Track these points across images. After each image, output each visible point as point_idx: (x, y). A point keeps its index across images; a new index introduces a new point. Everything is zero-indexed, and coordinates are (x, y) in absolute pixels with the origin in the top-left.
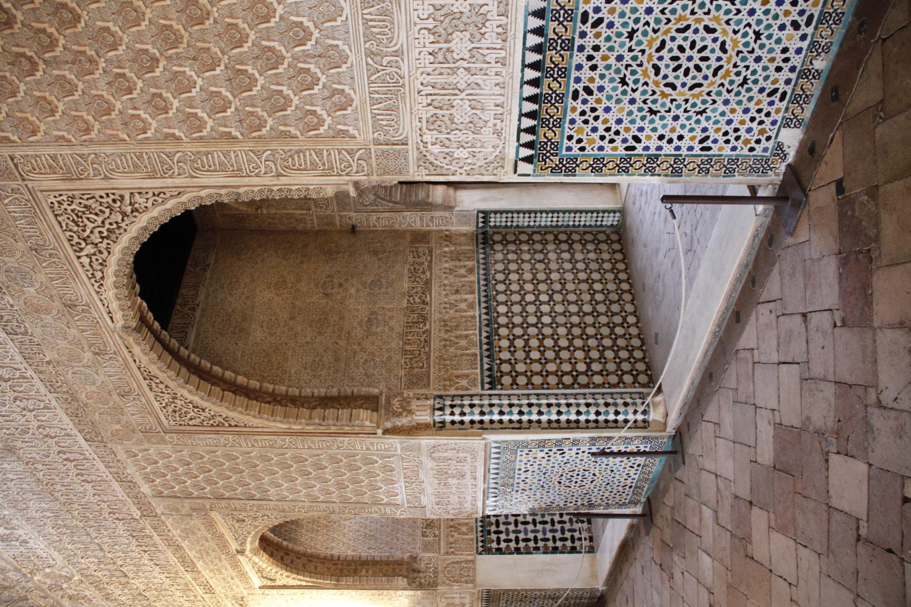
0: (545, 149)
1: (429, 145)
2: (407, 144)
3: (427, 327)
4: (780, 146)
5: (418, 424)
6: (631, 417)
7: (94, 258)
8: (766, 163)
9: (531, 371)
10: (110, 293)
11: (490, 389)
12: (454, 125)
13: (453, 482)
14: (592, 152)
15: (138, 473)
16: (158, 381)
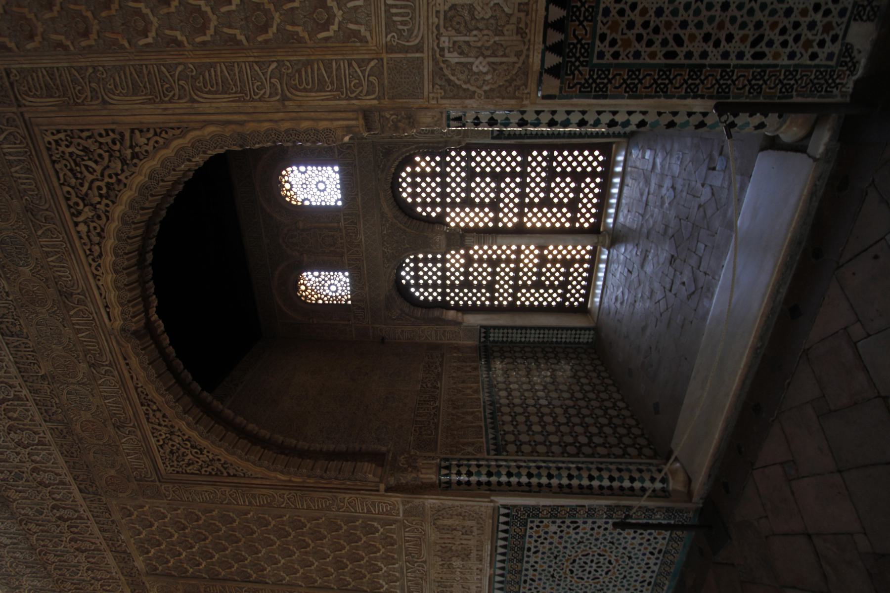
0: (574, 55)
1: (447, 54)
2: (422, 52)
3: (437, 404)
4: (848, 50)
5: (423, 483)
6: (648, 484)
7: (92, 225)
8: (831, 76)
9: (535, 441)
10: (109, 278)
11: (495, 455)
12: (473, 22)
13: (457, 563)
14: (626, 61)
15: (132, 541)
16: (155, 407)
